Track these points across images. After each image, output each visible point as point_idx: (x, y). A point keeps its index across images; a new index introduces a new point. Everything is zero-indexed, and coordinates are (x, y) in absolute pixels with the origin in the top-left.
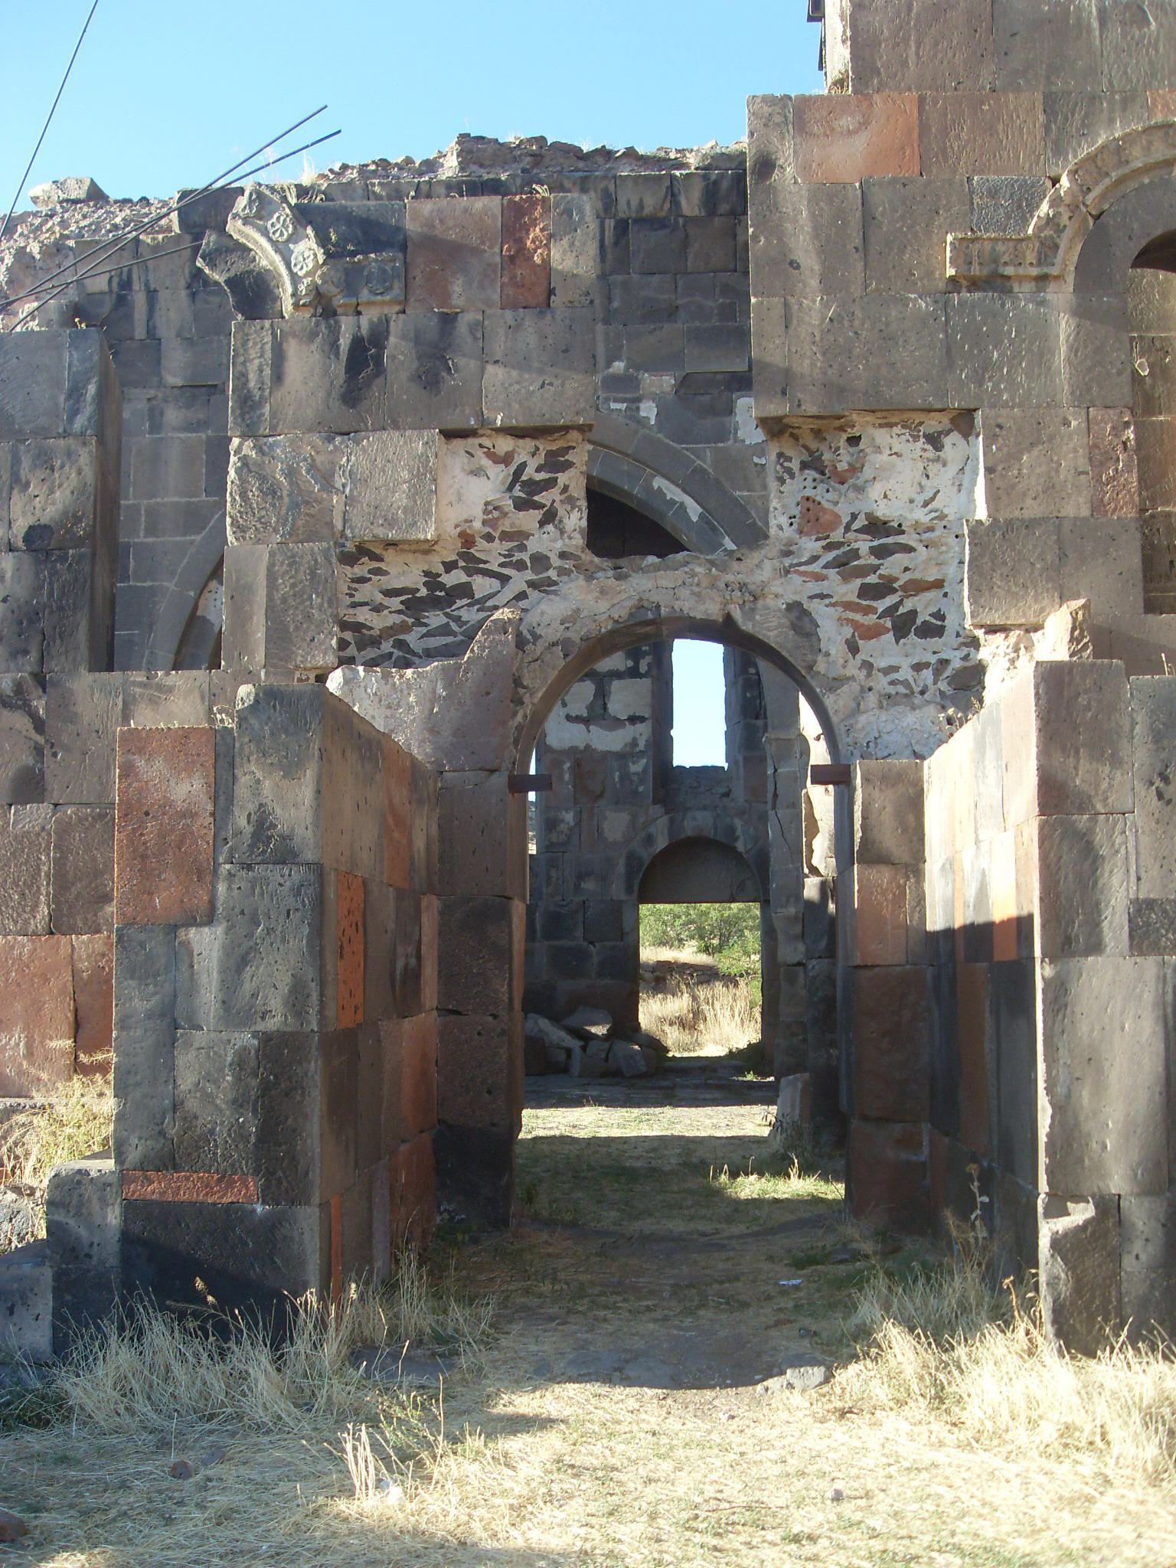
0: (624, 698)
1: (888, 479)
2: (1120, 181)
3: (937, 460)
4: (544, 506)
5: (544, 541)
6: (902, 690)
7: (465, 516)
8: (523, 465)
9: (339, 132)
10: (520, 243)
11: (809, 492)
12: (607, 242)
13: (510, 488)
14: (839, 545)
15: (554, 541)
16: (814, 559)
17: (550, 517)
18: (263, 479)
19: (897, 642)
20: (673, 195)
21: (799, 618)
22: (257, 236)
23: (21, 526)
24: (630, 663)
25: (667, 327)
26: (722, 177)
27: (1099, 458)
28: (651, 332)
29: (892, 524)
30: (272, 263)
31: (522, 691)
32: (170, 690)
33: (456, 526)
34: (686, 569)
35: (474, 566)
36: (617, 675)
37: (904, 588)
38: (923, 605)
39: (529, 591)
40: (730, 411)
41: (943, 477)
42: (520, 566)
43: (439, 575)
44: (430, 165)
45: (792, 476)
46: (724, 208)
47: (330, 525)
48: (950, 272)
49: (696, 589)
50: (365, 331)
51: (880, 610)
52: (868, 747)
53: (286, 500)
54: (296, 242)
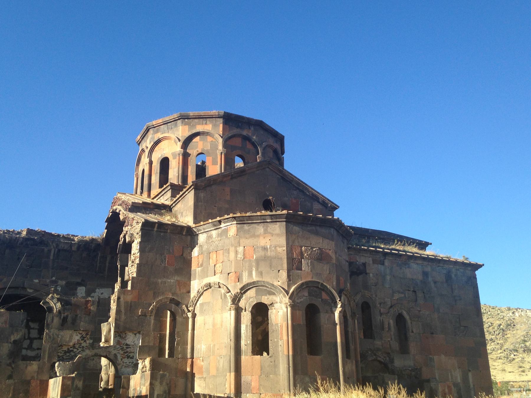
5: (84, 344)
6: (127, 365)
8: (83, 335)
10: (87, 306)
11: (119, 340)
12: (55, 253)
13: (81, 338)
15: (85, 344)
16: (118, 348)
17: (85, 341)
18: (49, 335)
20: (71, 246)
22: (51, 302)
23: (12, 340)
30: (53, 306)
32: (33, 364)
36: (36, 339)
38: (131, 355)
40: (76, 289)
41: (136, 339)
42: (80, 348)
44: (19, 233)
54: (57, 303)
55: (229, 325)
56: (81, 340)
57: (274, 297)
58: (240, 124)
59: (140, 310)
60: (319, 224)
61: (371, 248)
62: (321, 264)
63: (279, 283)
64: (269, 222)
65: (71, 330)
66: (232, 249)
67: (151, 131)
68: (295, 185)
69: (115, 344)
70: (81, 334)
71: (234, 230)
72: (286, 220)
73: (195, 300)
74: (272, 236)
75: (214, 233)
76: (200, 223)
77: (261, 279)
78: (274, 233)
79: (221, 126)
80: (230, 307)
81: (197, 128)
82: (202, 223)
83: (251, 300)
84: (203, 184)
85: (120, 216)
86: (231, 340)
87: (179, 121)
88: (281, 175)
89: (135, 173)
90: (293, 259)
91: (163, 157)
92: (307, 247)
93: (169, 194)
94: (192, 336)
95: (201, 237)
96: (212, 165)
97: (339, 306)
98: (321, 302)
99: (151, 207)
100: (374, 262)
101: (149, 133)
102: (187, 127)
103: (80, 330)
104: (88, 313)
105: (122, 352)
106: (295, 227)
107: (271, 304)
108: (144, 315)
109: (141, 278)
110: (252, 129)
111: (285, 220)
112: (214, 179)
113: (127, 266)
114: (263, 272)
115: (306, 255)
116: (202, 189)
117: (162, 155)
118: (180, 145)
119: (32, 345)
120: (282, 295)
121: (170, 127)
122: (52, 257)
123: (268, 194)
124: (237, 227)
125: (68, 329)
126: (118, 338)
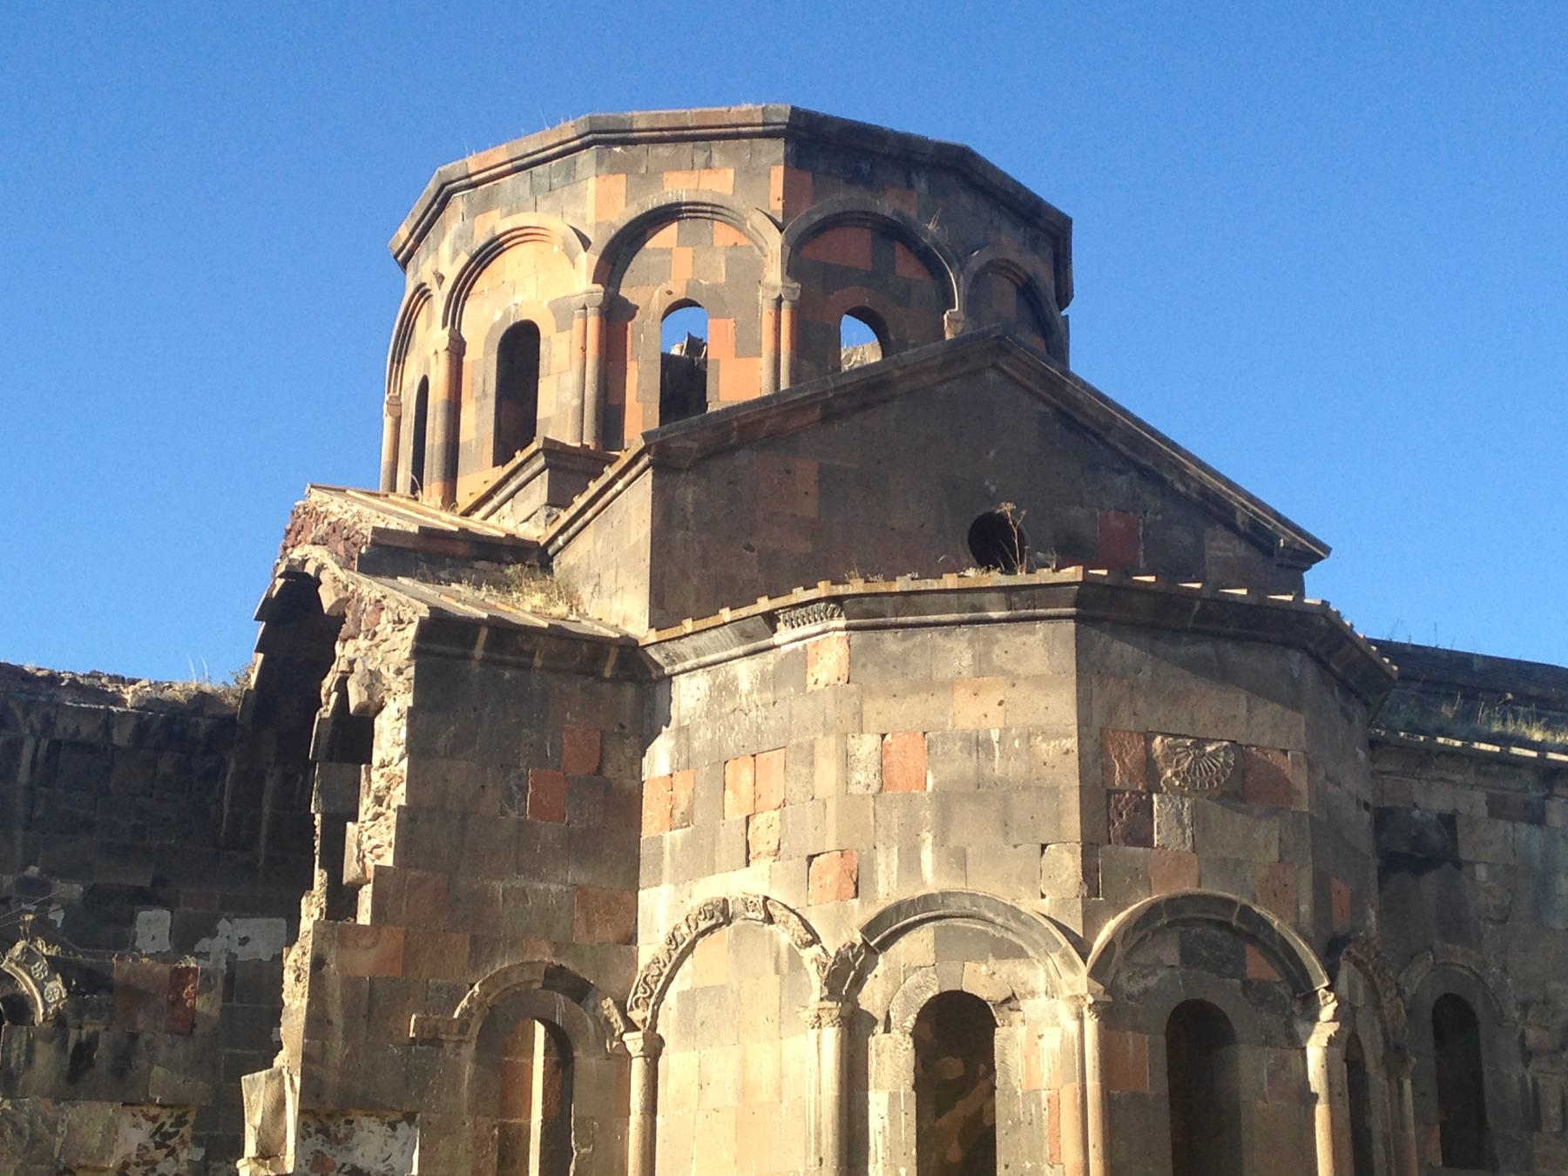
4: (169, 1146)
8: (164, 1123)
10: (179, 994)
11: (319, 1148)
13: (153, 1136)
17: (172, 1152)
22: (24, 974)
27: (479, 1143)
30: (31, 991)
40: (131, 920)
41: (395, 1147)
47: (52, 1155)
48: (412, 1035)
50: (84, 1037)
53: (28, 1138)
54: (49, 981)
55: (813, 1095)
57: (1018, 968)
58: (865, 167)
59: (414, 1016)
60: (1231, 630)
61: (1483, 746)
62: (1239, 817)
63: (1045, 905)
64: (998, 621)
65: (111, 1100)
66: (827, 746)
67: (459, 203)
68: (1120, 446)
71: (834, 659)
72: (1078, 613)
73: (660, 974)
74: (1014, 685)
75: (745, 672)
76: (681, 624)
77: (958, 886)
78: (1020, 671)
79: (778, 174)
80: (815, 1013)
81: (668, 188)
82: (688, 625)
83: (913, 979)
84: (695, 445)
85: (320, 590)
86: (821, 1160)
87: (586, 157)
88: (1055, 401)
89: (387, 398)
90: (1109, 793)
91: (512, 323)
92: (1176, 736)
93: (539, 490)
94: (644, 1139)
95: (683, 690)
96: (737, 356)
97: (1327, 1012)
98: (1240, 995)
99: (461, 549)
100: (1497, 808)
101: (448, 211)
102: (619, 183)
103: (151, 1102)
104: (187, 1025)
106: (1118, 646)
107: (1007, 1000)
108: (431, 1040)
109: (415, 873)
110: (922, 185)
111: (1072, 610)
112: (744, 421)
113: (355, 819)
114: (969, 851)
115: (1169, 773)
116: (688, 470)
117: (506, 315)
118: (589, 262)
120: (1055, 957)
121: (545, 182)
122: (23, 777)
123: (993, 489)
124: (848, 642)
125: (94, 1096)
126: (315, 1143)
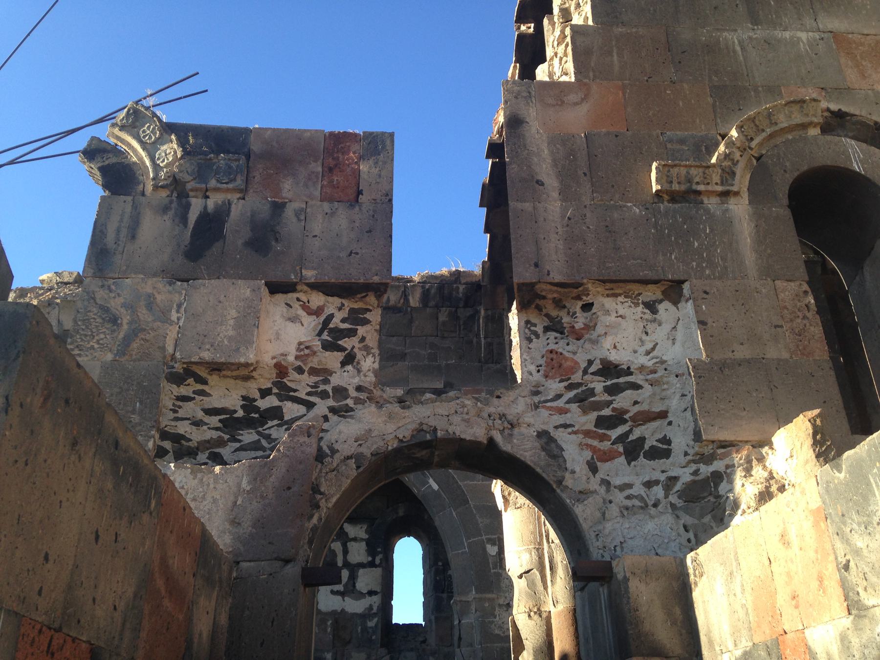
0: (366, 580)
1: (616, 335)
2: (771, 136)
3: (655, 320)
4: (345, 349)
5: (344, 378)
6: (637, 503)
7: (281, 351)
8: (331, 316)
9: (206, 91)
11: (552, 346)
13: (320, 334)
14: (579, 385)
15: (353, 377)
16: (558, 397)
17: (349, 359)
19: (629, 464)
20: (405, 296)
21: (547, 443)
24: (370, 559)
25: (400, 364)
26: (431, 287)
28: (391, 366)
29: (623, 367)
30: (141, 159)
31: (318, 497)
33: (273, 358)
34: (457, 401)
35: (286, 393)
37: (634, 419)
38: (650, 433)
39: (330, 415)
41: (659, 334)
42: (324, 395)
43: (255, 400)
45: (538, 336)
46: (432, 303)
47: (163, 349)
48: (655, 187)
49: (467, 417)
51: (613, 438)
52: (615, 550)
53: (125, 327)
54: (163, 144)
56: (317, 344)
59: (655, 165)
69: (537, 377)
70: (317, 312)
105: (584, 419)
119: (354, 583)
